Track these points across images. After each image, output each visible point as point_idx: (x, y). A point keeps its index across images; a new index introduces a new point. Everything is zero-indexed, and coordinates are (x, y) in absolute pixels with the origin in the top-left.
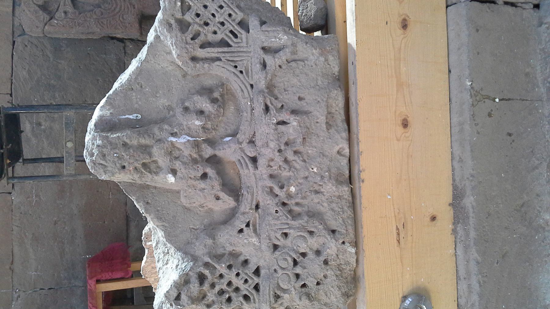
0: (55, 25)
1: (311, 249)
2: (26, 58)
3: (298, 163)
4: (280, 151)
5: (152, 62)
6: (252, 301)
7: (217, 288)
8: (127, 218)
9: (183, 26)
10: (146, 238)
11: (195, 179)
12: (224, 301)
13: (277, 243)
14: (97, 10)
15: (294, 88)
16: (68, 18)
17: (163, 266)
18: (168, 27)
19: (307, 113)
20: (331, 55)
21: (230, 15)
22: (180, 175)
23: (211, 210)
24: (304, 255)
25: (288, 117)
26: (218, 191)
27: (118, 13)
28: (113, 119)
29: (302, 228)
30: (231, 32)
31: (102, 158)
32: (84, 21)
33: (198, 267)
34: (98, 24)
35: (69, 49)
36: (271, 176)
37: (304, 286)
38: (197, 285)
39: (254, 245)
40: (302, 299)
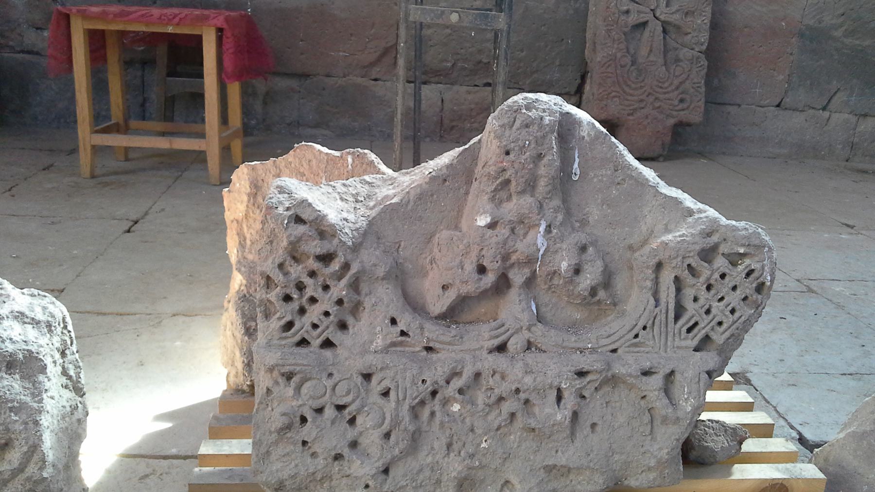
1: (361, 433)
3: (496, 418)
4: (518, 391)
5: (654, 203)
6: (284, 334)
7: (308, 281)
8: (305, 76)
9: (707, 254)
10: (358, 156)
11: (480, 256)
12: (288, 292)
13: (375, 380)
14: (628, 60)
15: (610, 418)
16: (619, 15)
17: (339, 193)
18: (707, 231)
19: (573, 434)
20: (657, 476)
21: (720, 324)
22: (488, 235)
23: (425, 275)
24: (352, 421)
25: (569, 407)
26: (459, 290)
27: (623, 90)
28: (574, 140)
29: (396, 422)
30: (696, 324)
31: (525, 122)
33: (344, 253)
35: (571, 12)
36: (478, 375)
37: (304, 420)
38: (319, 251)
39: (371, 342)
40: (284, 417)
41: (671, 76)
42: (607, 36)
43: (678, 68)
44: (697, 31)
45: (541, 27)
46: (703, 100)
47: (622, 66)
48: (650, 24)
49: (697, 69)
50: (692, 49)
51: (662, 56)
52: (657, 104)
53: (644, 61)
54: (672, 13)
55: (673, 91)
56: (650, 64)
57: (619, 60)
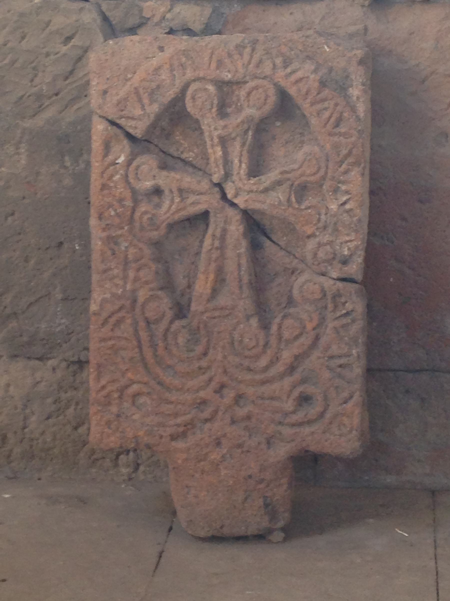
0: (110, 158)
2: (23, 38)
16: (136, 202)
32: (126, 257)
34: (116, 307)
35: (67, 182)
41: (273, 341)
42: (109, 253)
43: (289, 322)
44: (330, 230)
45: (6, 218)
46: (357, 397)
47: (148, 323)
48: (212, 219)
49: (337, 323)
50: (323, 274)
51: (246, 292)
52: (241, 412)
53: (201, 308)
54: (266, 190)
55: (282, 376)
56: (217, 314)
57: (143, 306)
